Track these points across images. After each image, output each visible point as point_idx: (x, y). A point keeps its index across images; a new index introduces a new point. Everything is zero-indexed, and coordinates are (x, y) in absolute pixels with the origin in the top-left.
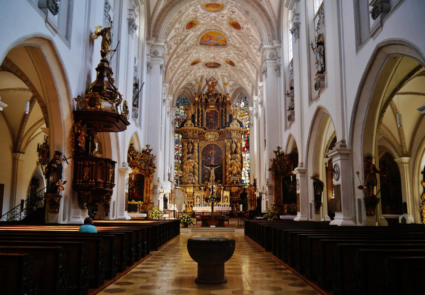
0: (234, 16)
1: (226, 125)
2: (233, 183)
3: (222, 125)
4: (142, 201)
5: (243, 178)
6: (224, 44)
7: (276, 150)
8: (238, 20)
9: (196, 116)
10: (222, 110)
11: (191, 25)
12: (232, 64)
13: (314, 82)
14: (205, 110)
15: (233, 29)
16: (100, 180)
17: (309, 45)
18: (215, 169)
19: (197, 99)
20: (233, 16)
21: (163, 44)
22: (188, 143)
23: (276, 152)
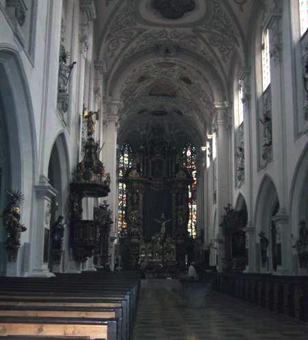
0: (186, 72)
1: (172, 174)
2: (179, 235)
3: (168, 175)
4: (100, 253)
5: (189, 230)
6: (174, 95)
7: (226, 206)
8: (189, 76)
9: (141, 164)
10: (168, 161)
11: (142, 79)
12: (179, 113)
13: (262, 153)
14: (151, 158)
15: (183, 83)
16: (92, 239)
17: (258, 120)
18: (166, 223)
19: (142, 147)
20: (184, 72)
21: (118, 102)
22: (133, 193)
23: (226, 209)
